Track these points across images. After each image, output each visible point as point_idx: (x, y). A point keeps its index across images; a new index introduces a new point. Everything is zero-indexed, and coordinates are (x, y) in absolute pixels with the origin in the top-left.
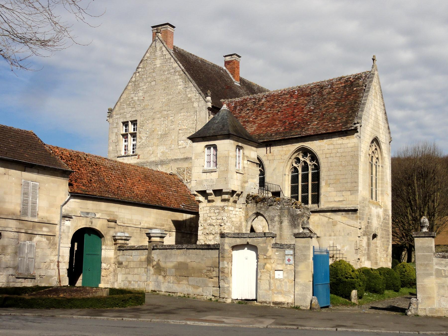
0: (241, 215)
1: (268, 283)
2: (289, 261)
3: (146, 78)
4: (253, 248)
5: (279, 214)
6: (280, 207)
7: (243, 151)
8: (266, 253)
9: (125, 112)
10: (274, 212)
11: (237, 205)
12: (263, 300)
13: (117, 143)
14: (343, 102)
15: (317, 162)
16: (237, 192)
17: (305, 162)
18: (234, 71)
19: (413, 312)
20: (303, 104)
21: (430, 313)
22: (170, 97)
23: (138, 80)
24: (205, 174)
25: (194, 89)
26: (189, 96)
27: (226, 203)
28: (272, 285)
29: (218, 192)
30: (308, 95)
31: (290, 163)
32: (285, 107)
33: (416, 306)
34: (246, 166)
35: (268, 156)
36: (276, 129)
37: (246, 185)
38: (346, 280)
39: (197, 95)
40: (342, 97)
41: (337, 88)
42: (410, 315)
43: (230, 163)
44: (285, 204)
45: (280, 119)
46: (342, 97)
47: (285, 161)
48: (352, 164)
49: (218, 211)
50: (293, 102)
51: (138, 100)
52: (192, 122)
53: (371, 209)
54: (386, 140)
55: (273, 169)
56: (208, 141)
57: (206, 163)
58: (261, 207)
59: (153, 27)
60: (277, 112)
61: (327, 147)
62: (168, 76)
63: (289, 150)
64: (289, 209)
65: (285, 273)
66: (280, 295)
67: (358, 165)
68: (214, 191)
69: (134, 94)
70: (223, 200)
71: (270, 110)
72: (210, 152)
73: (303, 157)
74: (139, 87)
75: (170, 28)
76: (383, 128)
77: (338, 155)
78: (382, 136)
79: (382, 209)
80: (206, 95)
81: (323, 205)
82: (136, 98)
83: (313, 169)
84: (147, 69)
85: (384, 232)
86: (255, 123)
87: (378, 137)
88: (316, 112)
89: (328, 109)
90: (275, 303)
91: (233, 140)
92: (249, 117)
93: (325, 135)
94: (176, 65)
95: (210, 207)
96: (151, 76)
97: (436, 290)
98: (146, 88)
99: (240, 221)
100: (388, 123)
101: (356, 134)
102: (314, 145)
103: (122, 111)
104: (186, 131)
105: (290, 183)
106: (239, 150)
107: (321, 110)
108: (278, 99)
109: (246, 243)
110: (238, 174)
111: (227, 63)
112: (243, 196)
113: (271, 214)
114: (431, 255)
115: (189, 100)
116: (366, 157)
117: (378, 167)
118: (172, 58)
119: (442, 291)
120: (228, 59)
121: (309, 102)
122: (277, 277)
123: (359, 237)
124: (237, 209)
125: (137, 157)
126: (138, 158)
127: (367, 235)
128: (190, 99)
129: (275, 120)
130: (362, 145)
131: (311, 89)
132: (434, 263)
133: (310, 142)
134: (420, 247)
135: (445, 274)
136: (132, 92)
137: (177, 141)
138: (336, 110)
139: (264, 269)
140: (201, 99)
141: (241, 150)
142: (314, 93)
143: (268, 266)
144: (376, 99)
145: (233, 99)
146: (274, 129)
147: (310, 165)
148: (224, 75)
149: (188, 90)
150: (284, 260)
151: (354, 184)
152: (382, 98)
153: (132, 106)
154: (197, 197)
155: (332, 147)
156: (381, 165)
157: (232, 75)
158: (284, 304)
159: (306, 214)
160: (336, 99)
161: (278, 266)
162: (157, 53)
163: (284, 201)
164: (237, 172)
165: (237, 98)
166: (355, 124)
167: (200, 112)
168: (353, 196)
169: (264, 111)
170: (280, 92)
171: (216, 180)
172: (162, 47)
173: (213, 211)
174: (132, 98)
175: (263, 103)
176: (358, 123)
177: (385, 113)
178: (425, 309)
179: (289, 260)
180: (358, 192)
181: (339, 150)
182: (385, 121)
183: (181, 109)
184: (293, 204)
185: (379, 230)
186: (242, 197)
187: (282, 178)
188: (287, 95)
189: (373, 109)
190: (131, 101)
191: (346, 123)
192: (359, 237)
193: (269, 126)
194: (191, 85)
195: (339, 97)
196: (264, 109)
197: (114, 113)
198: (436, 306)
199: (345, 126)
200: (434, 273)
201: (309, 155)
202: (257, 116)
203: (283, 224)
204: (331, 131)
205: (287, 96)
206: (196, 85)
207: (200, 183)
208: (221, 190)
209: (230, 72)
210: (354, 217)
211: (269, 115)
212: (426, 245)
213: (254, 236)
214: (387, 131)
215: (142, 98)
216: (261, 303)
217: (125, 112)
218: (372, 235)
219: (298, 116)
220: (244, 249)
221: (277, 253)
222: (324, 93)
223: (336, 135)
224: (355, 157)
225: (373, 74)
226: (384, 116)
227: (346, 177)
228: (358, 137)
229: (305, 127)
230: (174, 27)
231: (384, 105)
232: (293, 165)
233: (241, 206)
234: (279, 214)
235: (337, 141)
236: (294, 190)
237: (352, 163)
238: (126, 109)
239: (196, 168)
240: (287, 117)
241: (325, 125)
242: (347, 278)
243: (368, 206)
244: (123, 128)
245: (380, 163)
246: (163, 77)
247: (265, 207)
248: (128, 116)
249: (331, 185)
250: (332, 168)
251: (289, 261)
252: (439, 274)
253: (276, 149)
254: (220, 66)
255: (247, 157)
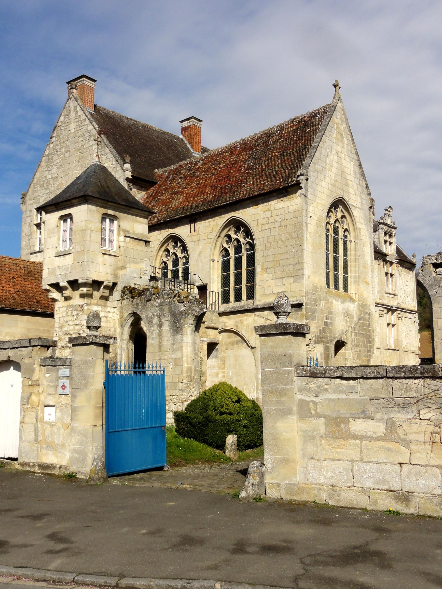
0: (115, 318)
1: (33, 429)
2: (63, 389)
3: (60, 149)
4: (17, 366)
5: (158, 312)
6: (159, 301)
7: (119, 223)
8: (32, 376)
9: (38, 196)
10: (153, 309)
11: (109, 303)
12: (27, 460)
13: (30, 236)
14: (290, 149)
15: (252, 239)
16: (105, 284)
17: (238, 241)
18: (193, 139)
19: (251, 490)
20: (242, 161)
21: (287, 493)
23: (51, 153)
24: (58, 258)
25: (110, 156)
27: (85, 301)
28: (40, 433)
29: (74, 284)
30: (251, 149)
31: (219, 244)
32: (222, 168)
33: (257, 478)
34: (122, 244)
35: (192, 236)
36: (204, 197)
37: (121, 272)
38: (218, 417)
39: (114, 163)
40: (290, 144)
41: (287, 133)
42: (244, 498)
43: (88, 239)
44: (165, 297)
45: (211, 184)
46: (290, 144)
47: (212, 240)
48: (294, 236)
49: (76, 312)
50: (232, 161)
51: (51, 178)
53: (332, 303)
54: (362, 204)
55: (198, 253)
56: (63, 209)
57: (61, 242)
58: (137, 304)
59: (68, 83)
60: (211, 175)
61: (263, 215)
62: (83, 143)
63: (217, 225)
64: (170, 304)
65: (58, 411)
66: (50, 452)
67: (303, 237)
68: (68, 282)
69: (47, 172)
70: (82, 296)
71: (204, 175)
72: (67, 227)
73: (236, 234)
74: (53, 162)
75: (87, 82)
76: (355, 186)
77: (277, 225)
78: (353, 197)
79: (356, 304)
80: (125, 163)
81: (260, 300)
82: (49, 177)
83: (247, 250)
84: (61, 137)
85: (361, 339)
86: (182, 193)
87: (345, 198)
88: (255, 169)
89: (270, 162)
90: (42, 466)
91: (96, 205)
92: (179, 187)
93: (260, 198)
94: (91, 127)
95: (67, 307)
96: (65, 145)
97: (298, 445)
98: (60, 162)
99: (114, 327)
100: (366, 180)
101: (299, 192)
102: (245, 215)
103: (35, 195)
105: (220, 272)
106: (112, 221)
107: (261, 164)
108: (216, 160)
109: (6, 359)
110: (106, 256)
111: (184, 130)
112: (118, 289)
113: (150, 314)
114: (289, 373)
116: (318, 225)
117: (348, 242)
118: (87, 119)
119: (311, 448)
120: (185, 124)
121: (249, 157)
122: (47, 418)
123: (307, 345)
124: (109, 309)
127: (322, 342)
129: (205, 186)
130: (311, 209)
131: (256, 140)
132: (296, 390)
133: (242, 211)
134: (270, 355)
135: (316, 410)
136: (46, 169)
138: (279, 162)
139: (28, 404)
140: (119, 168)
141: (116, 222)
142: (259, 145)
143: (34, 398)
144: (340, 144)
145: (168, 168)
146: (202, 198)
147: (243, 244)
148: (178, 145)
150: (56, 387)
151: (298, 266)
152: (353, 142)
153: (46, 187)
154: (51, 294)
155: (268, 214)
156: (353, 241)
157: (190, 144)
158: (54, 468)
159: (193, 310)
160: (283, 147)
161: (50, 397)
162: (71, 115)
163: (164, 292)
164: (103, 253)
165: (172, 166)
166: (298, 176)
168: (297, 284)
169: (197, 177)
170: (220, 150)
171: (71, 266)
172: (76, 107)
173: (70, 312)
174: (46, 177)
175: (199, 168)
176: (302, 175)
177: (360, 165)
178: (279, 485)
179: (64, 387)
180: (303, 278)
181: (278, 217)
182: (359, 176)
184: (175, 296)
185: (349, 334)
186: (117, 290)
187: (208, 266)
188: (227, 152)
189: (333, 157)
190: (44, 181)
191: (289, 177)
192: (307, 345)
193: (197, 196)
194: (107, 150)
195: (287, 145)
196: (198, 174)
197: (27, 198)
198: (299, 479)
199: (286, 181)
200: (295, 409)
201: (242, 230)
202: (188, 184)
203: (163, 328)
204: (266, 191)
205: (227, 154)
206: (113, 150)
207: (52, 272)
208: (77, 280)
209: (188, 140)
210: (299, 316)
211: (201, 181)
212: (280, 351)
213: (16, 346)
214: (365, 191)
215: (56, 176)
216: (22, 465)
217: (38, 196)
218: (334, 342)
219: (234, 177)
220: (8, 369)
221: (47, 375)
222: (270, 142)
223: (274, 196)
224: (298, 226)
225: (335, 107)
226: (357, 169)
227: (288, 257)
228: (302, 196)
229: (237, 191)
230: (94, 81)
231: (357, 153)
232: (223, 246)
233: (115, 304)
234: (158, 312)
235: (275, 204)
236: (225, 282)
237: (294, 235)
238: (39, 192)
239: (48, 250)
240: (220, 181)
241: (262, 184)
242: (221, 413)
243: (325, 299)
244: (37, 216)
245: (351, 237)
246: (78, 145)
247: (143, 304)
249: (268, 270)
250: (269, 244)
251: (63, 389)
252: (305, 411)
253: (201, 225)
254: (174, 133)
255: (125, 231)
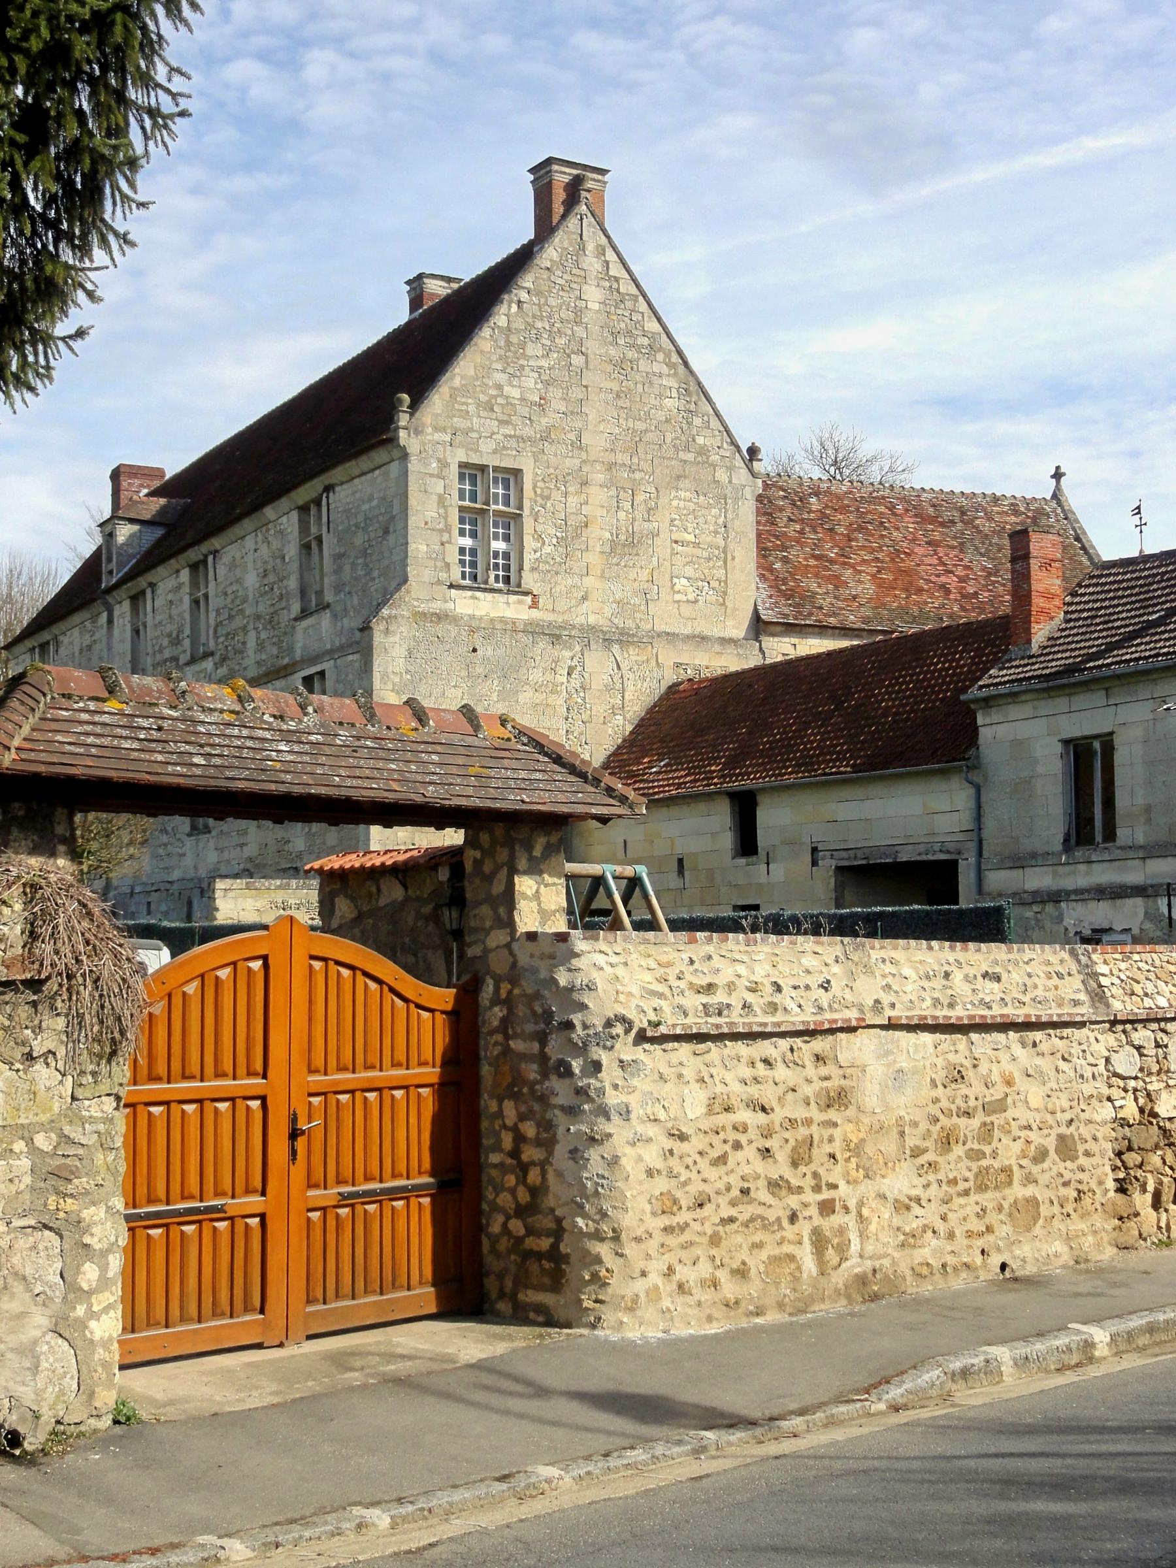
9: (471, 430)
22: (640, 426)
26: (700, 440)
51: (522, 399)
52: (712, 528)
104: (698, 552)
115: (700, 454)
125: (529, 599)
126: (534, 605)
128: (703, 451)
137: (667, 577)
149: (697, 421)
167: (736, 500)
174: (499, 387)
183: (678, 477)
190: (496, 397)
246: (612, 351)
248: (487, 446)
